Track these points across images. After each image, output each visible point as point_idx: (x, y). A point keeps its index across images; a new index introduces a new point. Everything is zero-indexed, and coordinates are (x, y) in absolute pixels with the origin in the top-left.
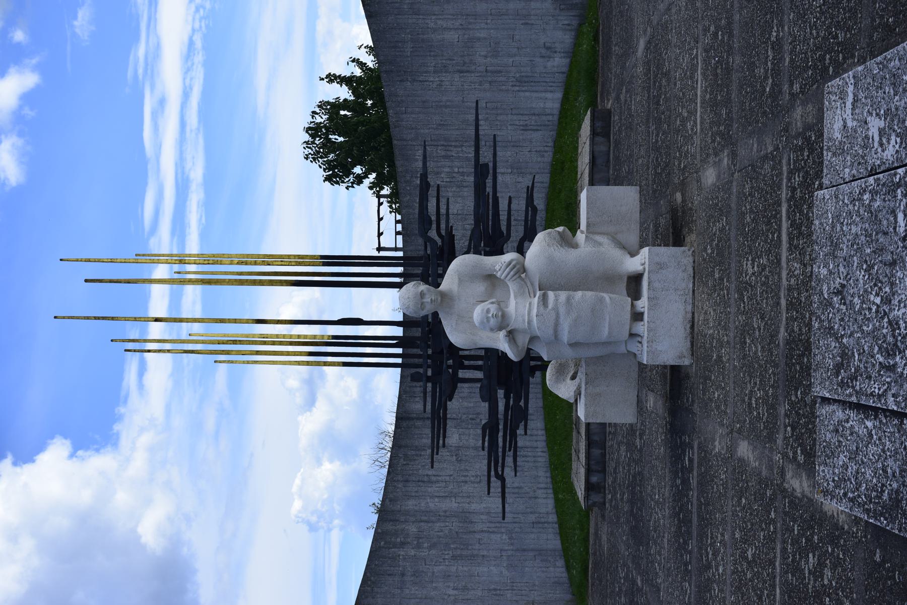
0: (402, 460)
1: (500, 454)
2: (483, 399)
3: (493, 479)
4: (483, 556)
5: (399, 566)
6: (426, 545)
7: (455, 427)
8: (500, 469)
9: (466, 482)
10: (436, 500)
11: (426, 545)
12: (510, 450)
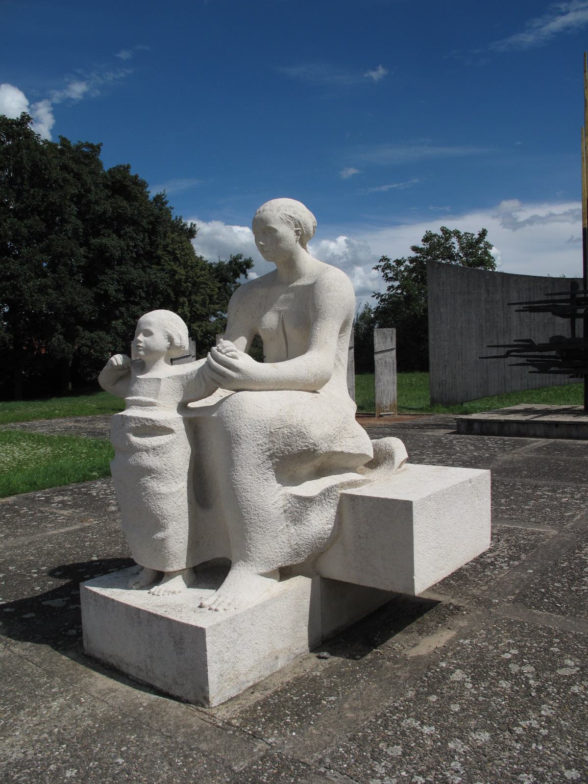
2: (552, 339)
3: (507, 349)
4: (482, 345)
9: (530, 330)
11: (488, 306)
12: (527, 360)
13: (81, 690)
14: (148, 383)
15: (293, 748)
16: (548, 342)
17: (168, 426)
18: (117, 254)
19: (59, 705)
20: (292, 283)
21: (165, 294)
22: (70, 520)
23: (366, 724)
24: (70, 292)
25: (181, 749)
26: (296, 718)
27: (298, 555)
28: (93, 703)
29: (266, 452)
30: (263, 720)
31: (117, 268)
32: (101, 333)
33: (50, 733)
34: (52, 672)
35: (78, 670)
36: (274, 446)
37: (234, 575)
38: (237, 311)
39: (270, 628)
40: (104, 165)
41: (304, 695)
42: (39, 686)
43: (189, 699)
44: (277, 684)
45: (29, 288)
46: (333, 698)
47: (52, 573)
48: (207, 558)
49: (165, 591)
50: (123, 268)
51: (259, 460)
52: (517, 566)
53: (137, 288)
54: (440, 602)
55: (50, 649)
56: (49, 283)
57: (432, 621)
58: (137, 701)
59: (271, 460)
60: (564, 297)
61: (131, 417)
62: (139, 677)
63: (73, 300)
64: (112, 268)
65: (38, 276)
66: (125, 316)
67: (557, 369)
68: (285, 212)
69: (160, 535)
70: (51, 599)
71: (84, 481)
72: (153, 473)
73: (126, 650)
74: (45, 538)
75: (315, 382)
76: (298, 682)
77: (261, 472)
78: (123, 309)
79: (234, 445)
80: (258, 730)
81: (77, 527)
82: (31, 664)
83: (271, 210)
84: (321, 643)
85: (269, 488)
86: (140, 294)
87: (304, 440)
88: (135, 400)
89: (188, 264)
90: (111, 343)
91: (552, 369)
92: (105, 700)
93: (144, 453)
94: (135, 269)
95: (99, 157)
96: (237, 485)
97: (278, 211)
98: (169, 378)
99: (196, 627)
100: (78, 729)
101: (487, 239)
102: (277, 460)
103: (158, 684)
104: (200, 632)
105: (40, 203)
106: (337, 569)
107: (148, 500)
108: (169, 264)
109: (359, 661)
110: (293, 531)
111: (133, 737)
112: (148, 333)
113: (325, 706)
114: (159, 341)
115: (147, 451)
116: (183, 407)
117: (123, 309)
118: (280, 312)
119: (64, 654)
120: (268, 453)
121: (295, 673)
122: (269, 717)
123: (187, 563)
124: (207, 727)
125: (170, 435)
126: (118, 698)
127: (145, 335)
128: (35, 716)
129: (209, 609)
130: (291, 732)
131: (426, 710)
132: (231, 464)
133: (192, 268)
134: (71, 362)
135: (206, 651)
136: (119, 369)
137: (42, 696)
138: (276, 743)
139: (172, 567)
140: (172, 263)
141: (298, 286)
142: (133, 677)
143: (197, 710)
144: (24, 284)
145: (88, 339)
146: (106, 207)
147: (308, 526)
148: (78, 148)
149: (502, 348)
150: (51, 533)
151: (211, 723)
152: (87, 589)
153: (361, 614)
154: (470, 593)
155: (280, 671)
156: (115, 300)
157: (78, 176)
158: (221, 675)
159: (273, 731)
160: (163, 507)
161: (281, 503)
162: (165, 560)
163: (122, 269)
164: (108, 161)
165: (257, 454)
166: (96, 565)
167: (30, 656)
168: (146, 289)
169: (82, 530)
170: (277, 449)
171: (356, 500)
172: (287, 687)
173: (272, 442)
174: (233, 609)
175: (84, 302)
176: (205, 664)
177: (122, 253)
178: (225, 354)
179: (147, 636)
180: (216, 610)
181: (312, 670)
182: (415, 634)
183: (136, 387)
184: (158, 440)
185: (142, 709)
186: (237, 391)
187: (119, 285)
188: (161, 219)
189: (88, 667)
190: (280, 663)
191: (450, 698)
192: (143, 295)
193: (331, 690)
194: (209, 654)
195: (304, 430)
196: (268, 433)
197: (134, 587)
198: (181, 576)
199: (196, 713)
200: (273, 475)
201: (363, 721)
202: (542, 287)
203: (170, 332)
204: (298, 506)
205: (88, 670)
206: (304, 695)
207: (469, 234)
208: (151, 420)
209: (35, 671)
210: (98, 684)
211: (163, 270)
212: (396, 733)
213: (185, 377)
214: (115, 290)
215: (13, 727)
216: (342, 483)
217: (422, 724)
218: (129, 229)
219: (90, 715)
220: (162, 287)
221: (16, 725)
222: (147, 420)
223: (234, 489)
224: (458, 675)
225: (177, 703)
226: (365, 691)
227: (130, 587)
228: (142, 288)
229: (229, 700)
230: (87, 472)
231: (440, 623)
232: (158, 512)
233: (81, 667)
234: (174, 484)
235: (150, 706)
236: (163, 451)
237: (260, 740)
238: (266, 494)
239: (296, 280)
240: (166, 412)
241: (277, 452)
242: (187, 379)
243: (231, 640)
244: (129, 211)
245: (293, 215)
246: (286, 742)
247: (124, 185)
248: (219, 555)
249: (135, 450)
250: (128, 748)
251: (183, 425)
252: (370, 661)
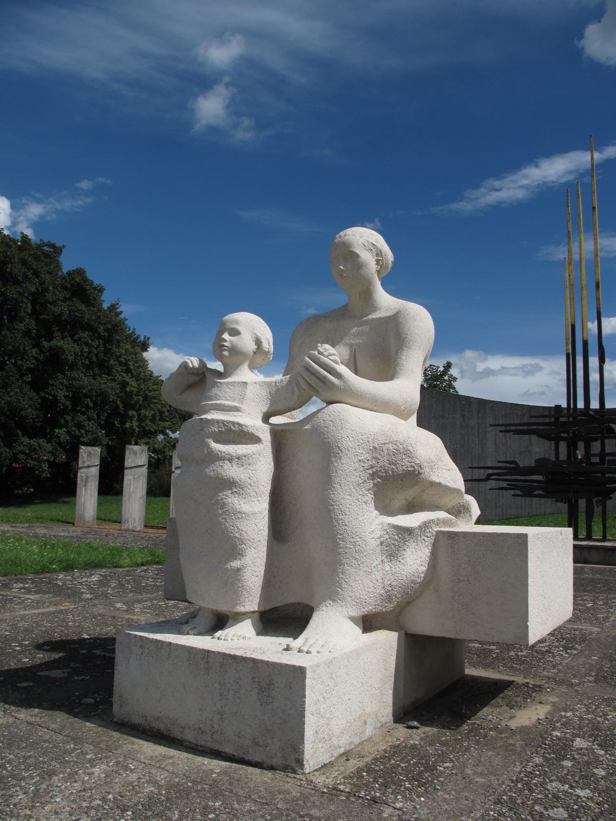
0: (520, 413)
1: (505, 477)
2: (536, 461)
5: (449, 414)
6: (463, 432)
7: (545, 450)
8: (494, 477)
10: (493, 438)
11: (463, 432)
12: (508, 484)
13: (125, 756)
14: (231, 387)
15: (431, 813)
16: (533, 464)
17: (256, 433)
18: (71, 358)
19: (102, 771)
20: (366, 316)
21: (114, 405)
22: (38, 604)
23: (506, 788)
24: (16, 394)
25: (287, 816)
26: (416, 783)
27: (389, 599)
28: (147, 770)
29: (367, 469)
30: (377, 785)
31: (68, 373)
32: (41, 440)
33: (104, 799)
34: (79, 738)
35: (111, 736)
36: (378, 463)
37: (320, 616)
38: (303, 342)
39: (362, 683)
40: (63, 267)
41: (412, 762)
42: (66, 752)
43: (274, 764)
44: (371, 752)
46: (448, 764)
47: (39, 647)
48: (277, 603)
49: (234, 635)
50: (75, 374)
51: (360, 479)
52: (576, 654)
53: (86, 396)
54: (514, 681)
55: (66, 716)
57: (517, 696)
58: (204, 768)
59: (372, 480)
60: (547, 420)
61: (213, 420)
62: (199, 744)
63: (19, 401)
64: (63, 373)
66: (70, 425)
67: (541, 492)
68: (368, 239)
69: (235, 564)
70: (47, 671)
71: (43, 572)
72: (235, 487)
73: (185, 708)
74: (17, 617)
75: (404, 411)
76: (396, 750)
77: (361, 493)
78: (68, 418)
79: (333, 459)
80: (376, 796)
81: (52, 609)
82: (46, 730)
83: (353, 235)
84: (402, 715)
85: (368, 513)
86: (88, 403)
87: (410, 460)
88: (217, 404)
89: (141, 376)
90: (50, 452)
91: (537, 492)
92: (162, 766)
93: (227, 462)
94: (85, 375)
95: (59, 259)
96: (333, 505)
97: (361, 237)
99: (294, 666)
100: (139, 795)
101: (453, 372)
102: (379, 480)
103: (228, 749)
104: (300, 672)
106: (427, 623)
107: (225, 519)
108: (120, 375)
109: (458, 731)
110: (388, 568)
111: (217, 804)
112: (235, 332)
113: (444, 772)
114: (246, 343)
115: (230, 460)
116: (266, 418)
117: (68, 418)
118: (351, 345)
119: (88, 721)
120: (370, 471)
121: (388, 742)
122: (381, 782)
123: (259, 604)
124: (310, 793)
125: (257, 445)
126: (178, 764)
127: (230, 335)
128: (76, 782)
129: (299, 652)
130: (419, 797)
131: (567, 774)
132: (327, 479)
133: (145, 380)
134: (5, 468)
135: (304, 696)
136: (193, 374)
137: (76, 762)
138: (406, 808)
139: (244, 606)
140: (124, 375)
141: (373, 319)
142: (190, 743)
143: (287, 776)
145: (27, 446)
146: (63, 308)
147: (404, 565)
148: (39, 247)
149: (482, 470)
150: (22, 613)
151: (313, 789)
152: (129, 634)
153: (442, 686)
154: (541, 675)
155: (368, 740)
156: (62, 407)
157: (36, 274)
158: (316, 732)
159: (396, 797)
160: (243, 529)
161: (378, 533)
162: (236, 596)
163: (72, 375)
164: (68, 263)
165: (358, 471)
166: (89, 643)
167: (42, 722)
168: (94, 399)
169: (61, 612)
170: (381, 467)
171: (456, 538)
172: (387, 755)
173: (376, 458)
174: (327, 652)
175: (29, 406)
176: (302, 715)
177: (75, 358)
178: (327, 357)
179: (217, 686)
180: (308, 652)
181: (406, 739)
182: (505, 708)
183: (215, 391)
184: (244, 449)
185: (216, 775)
186: (330, 403)
187: (68, 391)
188: (118, 327)
189: (124, 734)
190: (367, 730)
191: (588, 764)
192: (91, 404)
193: (442, 758)
194: (308, 700)
195: (410, 448)
196: (371, 448)
197: (191, 632)
198: (250, 620)
199: (288, 779)
200: (372, 498)
201: (500, 785)
202: (519, 415)
203: (258, 334)
204: (396, 537)
205: (125, 737)
206: (412, 762)
207: (435, 366)
208: (238, 424)
209: (54, 738)
210: (145, 750)
211: (114, 380)
212: (547, 796)
213: (274, 384)
214: (64, 396)
215: (49, 793)
216: (438, 519)
217: (571, 787)
218: (85, 334)
219: (149, 782)
220: (112, 397)
221: (53, 791)
222: (233, 423)
223: (329, 511)
224: (579, 743)
225: (257, 770)
226: (475, 764)
227: (185, 632)
228: (91, 398)
229: (322, 767)
230: (48, 564)
231: (527, 698)
232: (237, 535)
233: (116, 735)
234: (257, 502)
235: (224, 772)
236: (250, 461)
237: (386, 806)
238: (365, 521)
239: (370, 314)
240: (250, 418)
241: (380, 471)
242: (276, 386)
243: (327, 688)
244: (87, 316)
245: (375, 244)
246: (418, 807)
247: (80, 289)
248: (292, 600)
249: (216, 458)
250: (217, 815)
251: (270, 437)
252: (470, 731)
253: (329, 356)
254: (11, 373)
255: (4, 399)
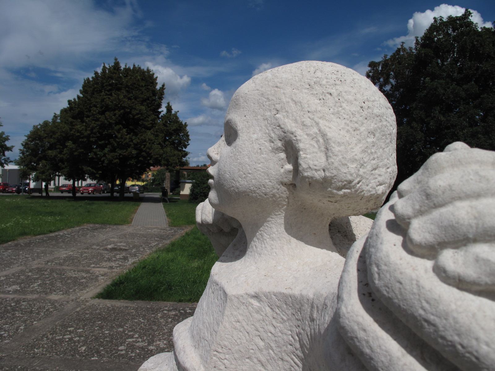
45: (463, 134)
56: (479, 130)
65: (471, 126)
98: (256, 297)
105: (475, 72)
144: (460, 131)
178: (429, 251)
203: (290, 125)
253: (443, 245)
254: (490, 123)
255: (487, 142)
